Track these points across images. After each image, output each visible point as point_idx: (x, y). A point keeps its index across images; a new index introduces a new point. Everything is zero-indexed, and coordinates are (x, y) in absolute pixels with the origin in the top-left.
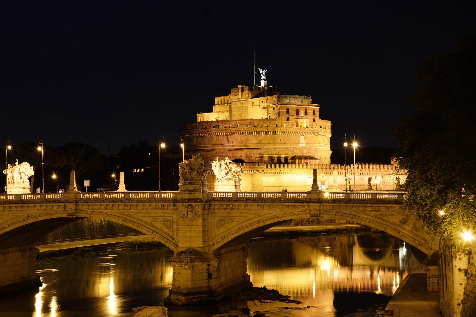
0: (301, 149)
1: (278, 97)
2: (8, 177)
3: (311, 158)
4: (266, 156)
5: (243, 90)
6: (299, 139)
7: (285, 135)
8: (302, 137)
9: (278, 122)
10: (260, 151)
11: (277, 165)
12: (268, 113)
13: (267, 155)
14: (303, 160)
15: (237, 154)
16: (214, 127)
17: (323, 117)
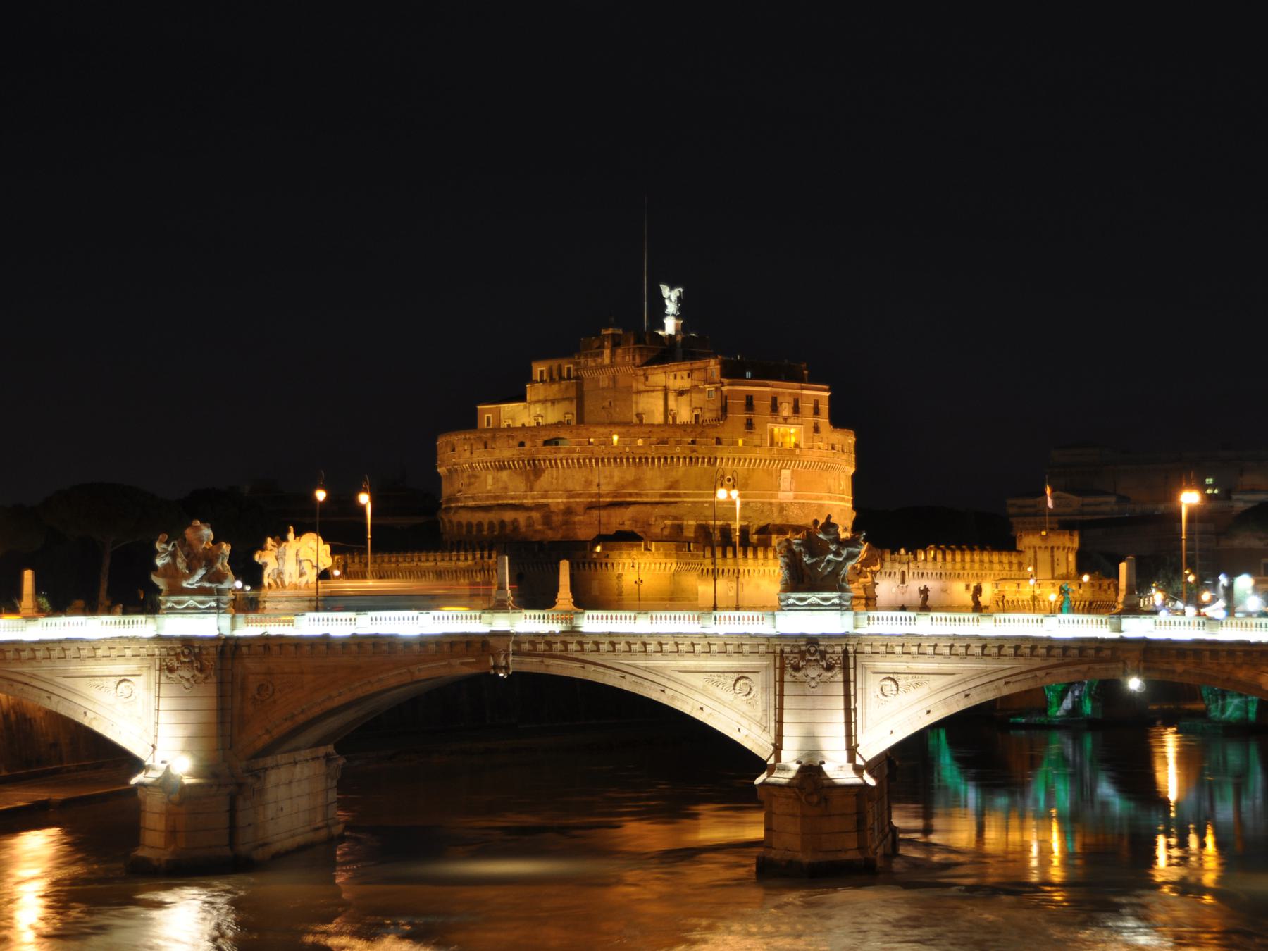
0: (782, 508)
2: (267, 572)
5: (616, 343)
8: (786, 473)
10: (672, 510)
13: (693, 523)
15: (609, 516)
16: (546, 443)
17: (838, 421)
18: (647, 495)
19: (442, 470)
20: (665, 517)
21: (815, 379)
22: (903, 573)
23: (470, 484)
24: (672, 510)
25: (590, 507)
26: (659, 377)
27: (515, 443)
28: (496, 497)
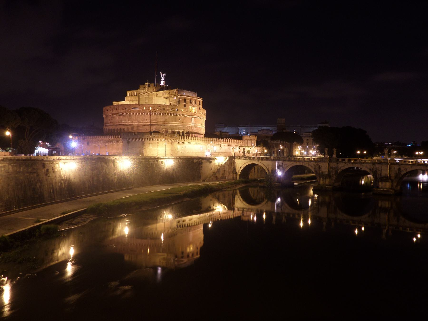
0: (192, 127)
1: (178, 91)
4: (170, 130)
5: (149, 86)
7: (183, 117)
8: (193, 119)
10: (165, 127)
11: (183, 137)
16: (132, 109)
17: (204, 108)
19: (104, 116)
21: (199, 96)
24: (165, 127)
25: (144, 125)
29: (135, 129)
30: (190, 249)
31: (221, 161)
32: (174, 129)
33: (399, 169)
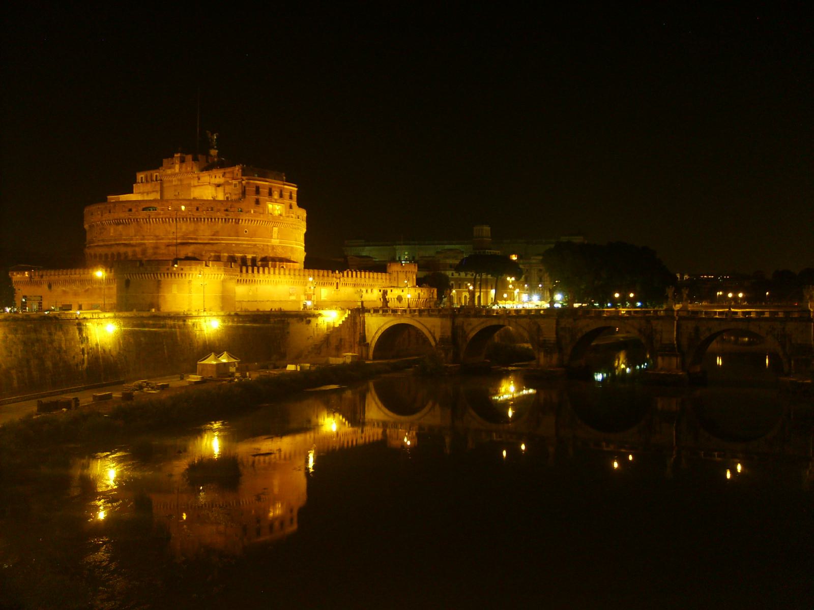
0: (273, 247)
3: (289, 261)
5: (182, 161)
6: (272, 232)
8: (275, 229)
9: (243, 205)
10: (215, 248)
12: (224, 192)
13: (226, 254)
14: (278, 263)
16: (143, 210)
17: (300, 204)
18: (201, 239)
19: (86, 226)
20: (212, 251)
21: (290, 180)
22: (337, 283)
23: (101, 233)
24: (215, 248)
25: (168, 245)
26: (206, 177)
27: (127, 210)
28: (115, 240)
29: (150, 251)
30: (276, 511)
31: (331, 318)
32: (234, 252)
33: (697, 329)
